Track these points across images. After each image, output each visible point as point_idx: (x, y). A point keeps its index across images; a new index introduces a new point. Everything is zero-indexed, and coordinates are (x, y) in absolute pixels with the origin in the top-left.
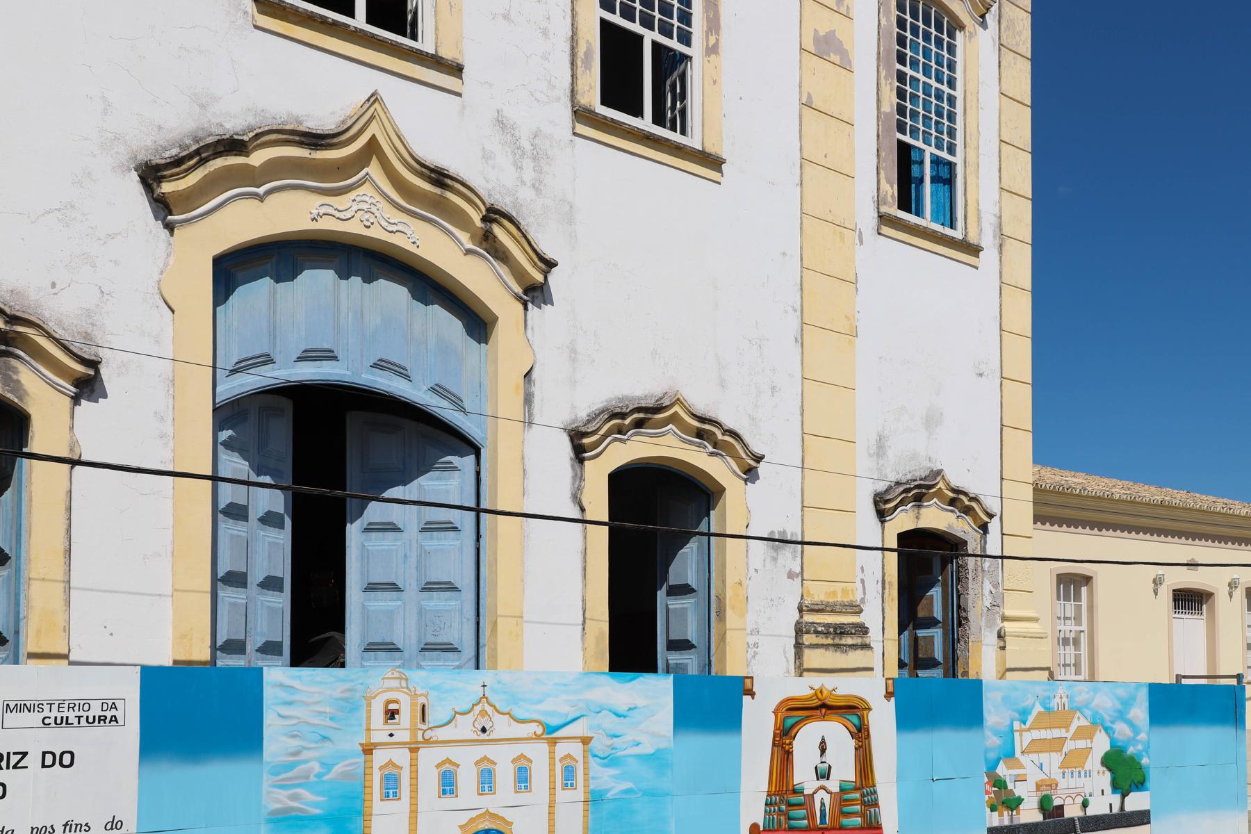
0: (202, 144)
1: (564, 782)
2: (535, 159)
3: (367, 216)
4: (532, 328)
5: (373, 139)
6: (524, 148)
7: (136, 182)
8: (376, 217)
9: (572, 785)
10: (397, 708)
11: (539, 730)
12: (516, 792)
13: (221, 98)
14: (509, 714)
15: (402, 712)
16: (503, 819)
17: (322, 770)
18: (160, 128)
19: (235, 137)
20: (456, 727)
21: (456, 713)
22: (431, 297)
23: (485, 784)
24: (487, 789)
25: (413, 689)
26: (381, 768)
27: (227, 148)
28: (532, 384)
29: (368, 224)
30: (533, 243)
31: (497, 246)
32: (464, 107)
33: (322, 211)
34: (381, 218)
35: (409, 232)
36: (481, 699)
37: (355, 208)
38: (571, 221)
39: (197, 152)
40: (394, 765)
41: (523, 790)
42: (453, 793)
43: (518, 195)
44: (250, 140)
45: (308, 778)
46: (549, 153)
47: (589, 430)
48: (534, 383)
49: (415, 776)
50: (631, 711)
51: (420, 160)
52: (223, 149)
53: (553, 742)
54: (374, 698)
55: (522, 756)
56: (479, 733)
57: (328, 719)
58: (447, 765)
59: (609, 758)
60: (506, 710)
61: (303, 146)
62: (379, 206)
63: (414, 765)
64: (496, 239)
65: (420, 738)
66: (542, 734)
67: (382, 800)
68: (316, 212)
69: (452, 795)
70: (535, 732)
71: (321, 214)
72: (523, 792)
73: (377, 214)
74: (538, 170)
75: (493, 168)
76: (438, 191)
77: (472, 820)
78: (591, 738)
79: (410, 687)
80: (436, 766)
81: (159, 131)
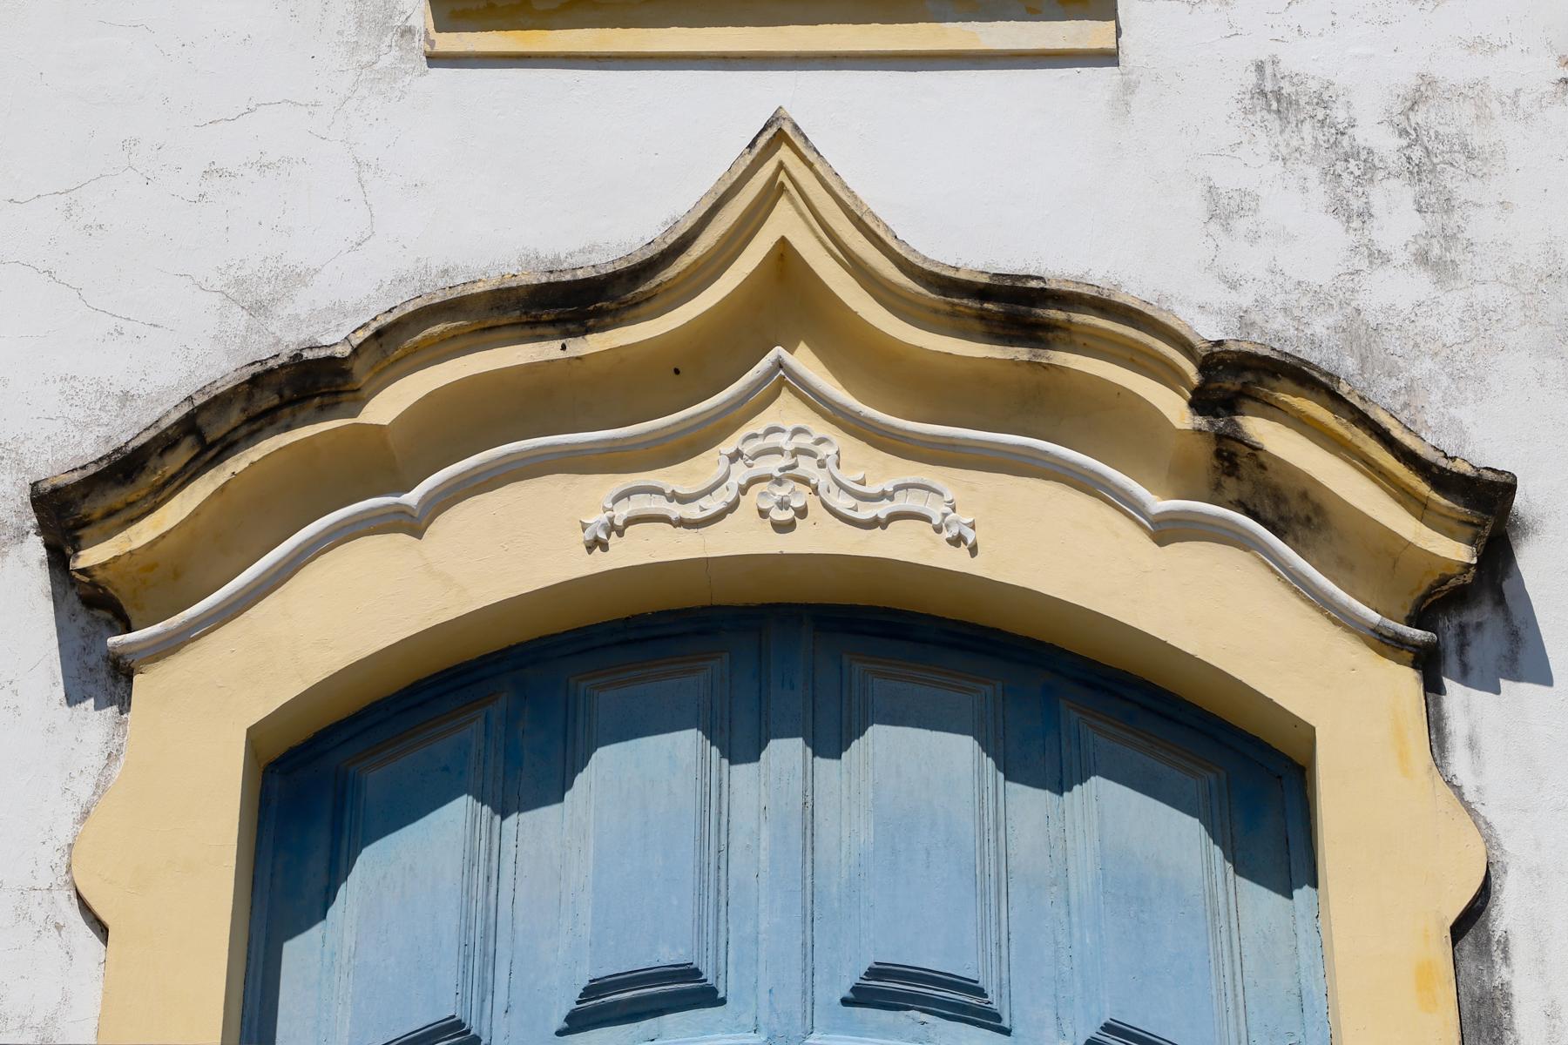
0: (199, 401)
2: (1416, 172)
3: (781, 492)
4: (1472, 744)
5: (783, 252)
6: (1370, 152)
8: (815, 490)
19: (308, 355)
22: (1075, 715)
27: (287, 393)
28: (1497, 956)
29: (787, 515)
30: (1397, 433)
31: (1276, 480)
32: (1129, 88)
33: (622, 512)
35: (935, 510)
37: (740, 473)
39: (189, 425)
43: (1361, 300)
44: (356, 351)
46: (1476, 141)
48: (1505, 951)
51: (911, 258)
61: (540, 331)
62: (823, 450)
64: (1263, 458)
68: (603, 518)
71: (619, 522)
73: (820, 477)
75: (1254, 238)
76: (1022, 353)
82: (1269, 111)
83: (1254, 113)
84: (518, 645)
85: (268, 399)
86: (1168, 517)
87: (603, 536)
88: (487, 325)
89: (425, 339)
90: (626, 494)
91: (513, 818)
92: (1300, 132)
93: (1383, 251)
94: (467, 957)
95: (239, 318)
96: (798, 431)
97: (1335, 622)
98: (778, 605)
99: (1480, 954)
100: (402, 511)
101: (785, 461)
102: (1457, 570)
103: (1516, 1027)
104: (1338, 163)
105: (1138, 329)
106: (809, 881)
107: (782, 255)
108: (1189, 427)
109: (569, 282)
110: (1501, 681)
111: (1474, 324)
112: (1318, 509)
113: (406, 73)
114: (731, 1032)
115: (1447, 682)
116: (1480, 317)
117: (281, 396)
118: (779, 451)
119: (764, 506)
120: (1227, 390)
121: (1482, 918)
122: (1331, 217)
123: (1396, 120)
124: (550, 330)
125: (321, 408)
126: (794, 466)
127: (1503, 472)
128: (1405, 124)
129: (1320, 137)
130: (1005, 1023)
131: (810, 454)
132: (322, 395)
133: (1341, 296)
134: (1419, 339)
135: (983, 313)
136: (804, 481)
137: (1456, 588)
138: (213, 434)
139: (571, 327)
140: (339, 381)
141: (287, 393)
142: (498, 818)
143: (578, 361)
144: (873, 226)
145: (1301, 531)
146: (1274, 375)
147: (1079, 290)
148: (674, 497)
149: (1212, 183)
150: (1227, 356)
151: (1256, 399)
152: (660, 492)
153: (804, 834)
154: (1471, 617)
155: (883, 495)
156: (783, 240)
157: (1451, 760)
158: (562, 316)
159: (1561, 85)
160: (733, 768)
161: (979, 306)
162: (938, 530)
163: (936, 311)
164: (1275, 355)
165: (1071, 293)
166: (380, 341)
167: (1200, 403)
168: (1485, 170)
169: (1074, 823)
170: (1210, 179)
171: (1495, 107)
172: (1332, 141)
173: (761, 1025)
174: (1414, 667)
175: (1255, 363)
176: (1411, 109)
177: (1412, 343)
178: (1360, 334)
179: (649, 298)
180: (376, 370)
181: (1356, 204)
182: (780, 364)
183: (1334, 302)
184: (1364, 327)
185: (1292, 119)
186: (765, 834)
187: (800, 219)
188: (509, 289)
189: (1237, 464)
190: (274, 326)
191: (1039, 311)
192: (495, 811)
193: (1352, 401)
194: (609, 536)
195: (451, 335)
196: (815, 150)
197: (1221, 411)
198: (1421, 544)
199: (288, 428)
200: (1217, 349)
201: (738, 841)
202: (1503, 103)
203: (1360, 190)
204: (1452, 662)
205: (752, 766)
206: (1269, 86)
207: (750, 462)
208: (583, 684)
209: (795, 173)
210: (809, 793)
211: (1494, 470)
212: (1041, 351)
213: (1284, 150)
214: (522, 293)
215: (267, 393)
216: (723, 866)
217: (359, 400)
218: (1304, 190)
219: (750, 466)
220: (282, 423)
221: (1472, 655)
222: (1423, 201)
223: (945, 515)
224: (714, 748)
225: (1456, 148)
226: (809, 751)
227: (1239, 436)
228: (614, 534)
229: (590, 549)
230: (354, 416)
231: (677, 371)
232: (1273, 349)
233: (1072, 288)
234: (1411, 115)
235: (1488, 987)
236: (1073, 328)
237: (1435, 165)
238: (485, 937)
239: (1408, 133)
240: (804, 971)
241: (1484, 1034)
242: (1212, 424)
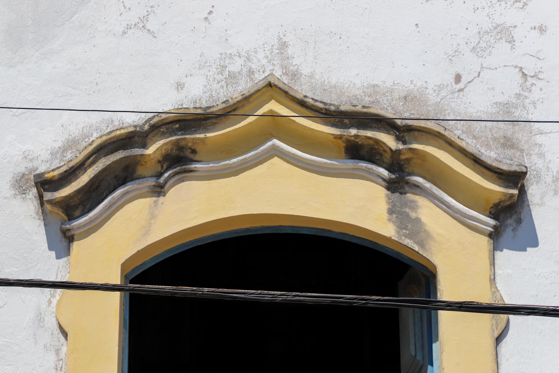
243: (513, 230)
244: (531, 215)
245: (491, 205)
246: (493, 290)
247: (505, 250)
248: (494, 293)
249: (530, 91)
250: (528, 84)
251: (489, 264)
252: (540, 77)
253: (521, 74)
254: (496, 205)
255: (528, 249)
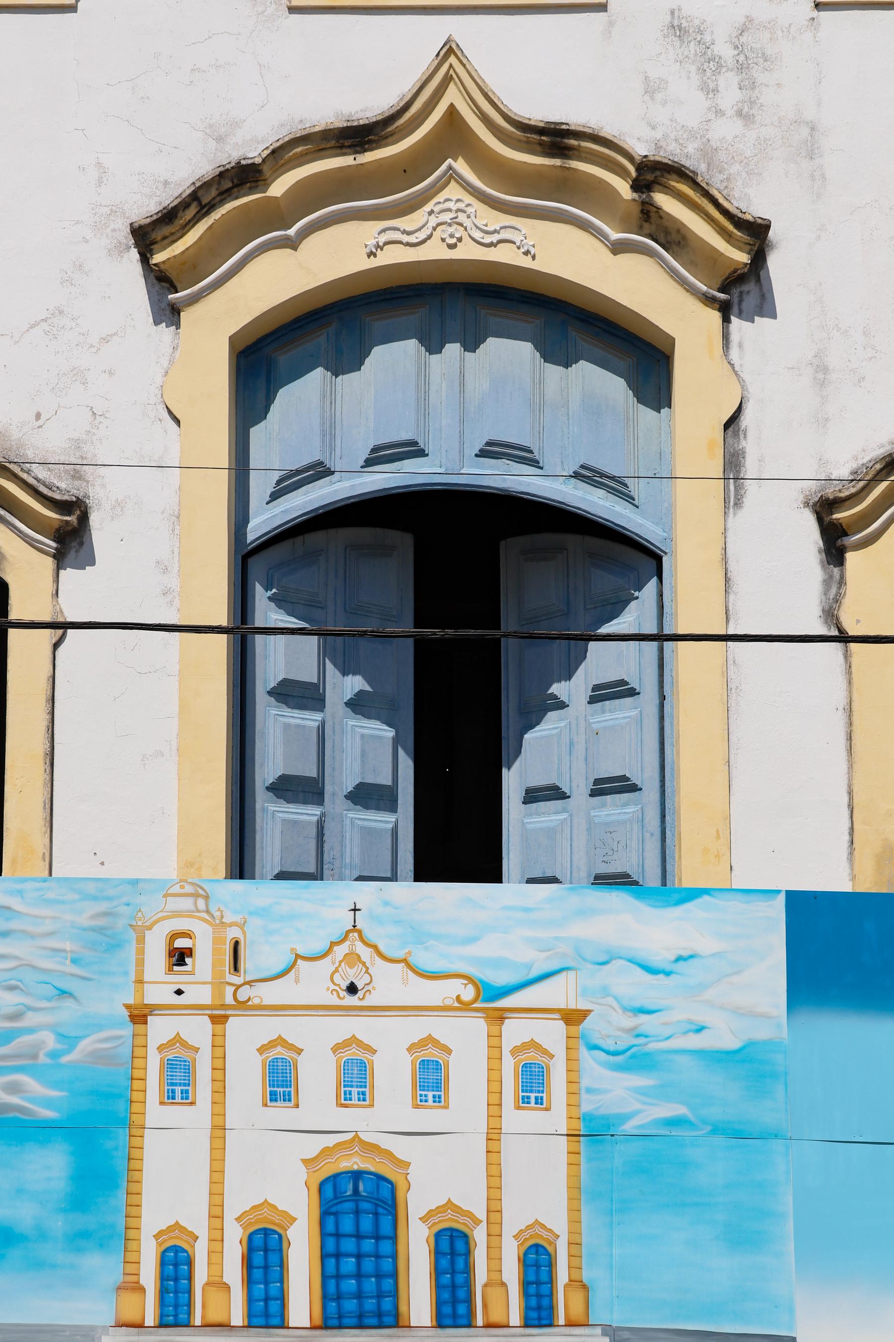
0: (198, 185)
1: (521, 1094)
2: (741, 68)
3: (451, 230)
4: (740, 345)
5: (452, 110)
6: (720, 58)
7: (136, 262)
8: (466, 229)
9: (539, 1101)
10: (190, 946)
11: (468, 994)
12: (416, 1107)
13: (244, 121)
14: (405, 961)
15: (197, 953)
16: (388, 1154)
17: (59, 1047)
18: (166, 183)
19: (243, 162)
20: (297, 981)
21: (298, 956)
22: (574, 333)
23: (352, 1086)
24: (355, 1096)
25: (217, 914)
26: (161, 1048)
28: (742, 436)
29: (453, 241)
30: (721, 201)
32: (611, 24)
33: (382, 239)
34: (474, 228)
35: (517, 238)
36: (348, 932)
37: (433, 221)
38: (811, 151)
39: (194, 196)
40: (184, 1044)
41: (430, 1102)
42: (290, 1100)
43: (710, 135)
44: (264, 160)
45: (35, 1057)
46: (768, 52)
47: (842, 495)
48: (745, 434)
49: (221, 1066)
50: (681, 963)
52: (230, 185)
53: (498, 1017)
54: (150, 928)
55: (429, 1041)
56: (343, 994)
57: (68, 962)
58: (279, 1049)
59: (629, 1053)
60: (400, 954)
61: (344, 150)
62: (470, 210)
63: (219, 1045)
64: (661, 213)
65: (229, 1000)
66: (475, 1000)
67: (161, 1103)
68: (374, 242)
69: (287, 1104)
70: (458, 997)
71: (381, 244)
72: (431, 1108)
73: (467, 223)
74: (749, 85)
75: (664, 103)
76: (557, 162)
77: (326, 1152)
78: (584, 1014)
79: (213, 909)
80: (258, 1050)
81: (165, 187)
82: (675, 36)
83: (668, 37)
84: (340, 300)
85: (228, 184)
86: (619, 241)
87: (374, 250)
88: (321, 148)
89: (294, 154)
90: (384, 231)
91: (341, 376)
92: (689, 47)
93: (722, 110)
94: (324, 436)
95: (212, 144)
96: (458, 200)
97: (687, 291)
98: (450, 283)
99: (735, 435)
100: (288, 238)
101: (452, 215)
102: (741, 266)
103: (746, 465)
104: (705, 64)
105: (610, 149)
106: (462, 405)
107: (451, 112)
108: (630, 199)
109: (356, 126)
110: (755, 317)
111: (759, 146)
112: (684, 238)
113: (279, 17)
114: (431, 467)
115: (732, 318)
116: (762, 143)
117: (233, 182)
118: (450, 210)
119: (443, 237)
120: (648, 180)
121: (737, 421)
122: (700, 92)
123: (733, 40)
124: (348, 150)
125: (250, 188)
126: (456, 218)
127: (766, 219)
128: (737, 43)
129: (698, 50)
130: (541, 465)
131: (464, 212)
132: (250, 182)
133: (702, 133)
134: (734, 154)
135: (542, 142)
136: (461, 225)
137: (741, 274)
138: (205, 201)
139: (358, 149)
140: (257, 175)
141: (235, 181)
142: (334, 377)
143: (362, 166)
144: (492, 97)
145: (675, 248)
146: (669, 172)
147: (584, 130)
148: (405, 232)
149: (647, 75)
150: (649, 163)
151: (660, 184)
152: (398, 229)
153: (460, 385)
154: (745, 288)
155: (495, 232)
156: (452, 104)
157: (731, 353)
158: (353, 143)
159: (811, 21)
160: (431, 356)
161: (539, 138)
162: (519, 248)
163: (520, 141)
164: (670, 163)
165: (581, 132)
166: (274, 155)
167: (636, 186)
168: (772, 67)
169: (572, 381)
170: (646, 72)
171: (779, 33)
172: (703, 52)
173: (443, 465)
174: (719, 311)
175: (661, 166)
176: (741, 34)
177: (731, 156)
178: (708, 152)
179: (392, 134)
180: (273, 169)
181: (712, 85)
182: (450, 168)
183: (698, 136)
184: (710, 149)
185: (686, 41)
186: (444, 385)
187: (459, 94)
188: (330, 130)
189: (650, 216)
190: (228, 148)
191: (566, 141)
192: (333, 374)
193: (702, 185)
194: (377, 250)
195: (305, 153)
196: (466, 57)
197: (644, 190)
198: (727, 254)
199: (237, 198)
200: (644, 160)
201: (433, 388)
202: (783, 31)
203: (714, 78)
204: (735, 309)
205: (439, 355)
206: (676, 23)
207: (437, 215)
208: (367, 319)
209: (457, 70)
210: (462, 367)
211: (762, 218)
212: (566, 161)
213: (681, 57)
214: (336, 131)
215: (226, 181)
216: (427, 399)
217: (267, 186)
218: (689, 78)
219: (437, 217)
220: (233, 196)
221: (744, 305)
222: (742, 84)
223: (522, 241)
224: (423, 347)
225: (760, 55)
226: (462, 349)
227: (652, 203)
228: (379, 249)
229: (369, 256)
230: (265, 192)
231: (405, 171)
232: (669, 159)
233: (581, 129)
234: (741, 37)
235: (737, 449)
236: (581, 149)
237: (749, 64)
238: (331, 427)
239: (738, 48)
240: (460, 442)
241: (733, 468)
242: (640, 197)
243: (76, 551)
244: (91, 539)
245: (54, 530)
246: (54, 603)
247: (68, 569)
248: (54, 606)
249: (98, 428)
250: (97, 422)
251: (52, 581)
252: (107, 416)
253: (91, 413)
254: (58, 530)
255: (87, 567)
